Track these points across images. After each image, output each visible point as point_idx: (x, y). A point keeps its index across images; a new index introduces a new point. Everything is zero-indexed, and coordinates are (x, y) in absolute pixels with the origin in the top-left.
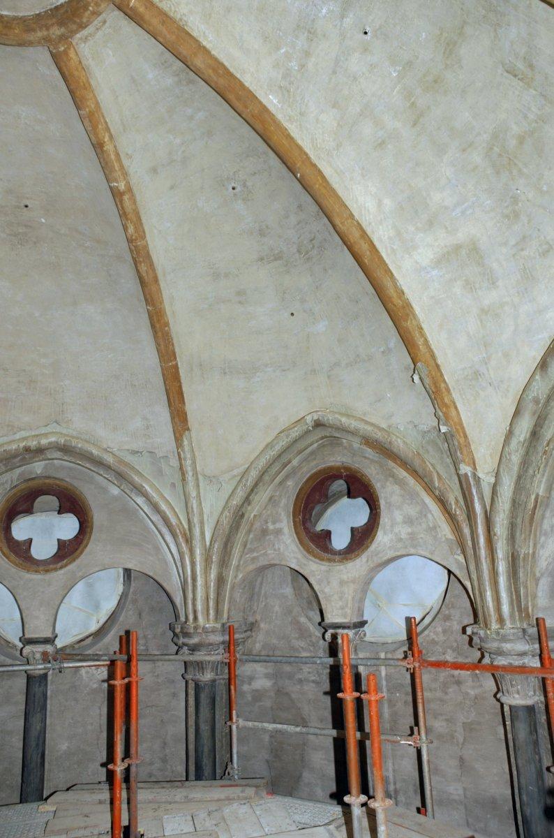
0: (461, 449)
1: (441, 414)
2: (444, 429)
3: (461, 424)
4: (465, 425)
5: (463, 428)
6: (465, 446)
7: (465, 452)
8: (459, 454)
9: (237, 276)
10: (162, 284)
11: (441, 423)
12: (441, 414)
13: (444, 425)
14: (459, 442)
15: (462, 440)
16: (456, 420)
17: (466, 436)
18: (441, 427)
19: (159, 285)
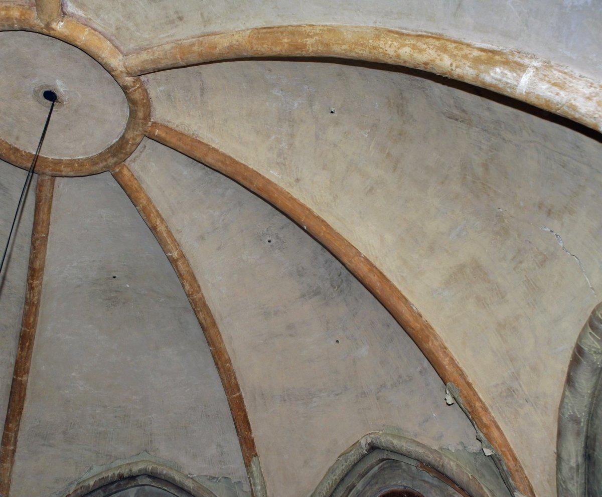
0: (512, 476)
1: (482, 435)
2: (488, 452)
3: (507, 445)
4: (512, 446)
5: (510, 450)
6: (517, 471)
7: (517, 478)
8: (510, 480)
9: (285, 312)
10: (221, 327)
11: (484, 445)
12: (482, 435)
13: (487, 447)
14: (508, 467)
15: (511, 464)
16: (499, 441)
17: (515, 459)
18: (485, 450)
19: (217, 328)
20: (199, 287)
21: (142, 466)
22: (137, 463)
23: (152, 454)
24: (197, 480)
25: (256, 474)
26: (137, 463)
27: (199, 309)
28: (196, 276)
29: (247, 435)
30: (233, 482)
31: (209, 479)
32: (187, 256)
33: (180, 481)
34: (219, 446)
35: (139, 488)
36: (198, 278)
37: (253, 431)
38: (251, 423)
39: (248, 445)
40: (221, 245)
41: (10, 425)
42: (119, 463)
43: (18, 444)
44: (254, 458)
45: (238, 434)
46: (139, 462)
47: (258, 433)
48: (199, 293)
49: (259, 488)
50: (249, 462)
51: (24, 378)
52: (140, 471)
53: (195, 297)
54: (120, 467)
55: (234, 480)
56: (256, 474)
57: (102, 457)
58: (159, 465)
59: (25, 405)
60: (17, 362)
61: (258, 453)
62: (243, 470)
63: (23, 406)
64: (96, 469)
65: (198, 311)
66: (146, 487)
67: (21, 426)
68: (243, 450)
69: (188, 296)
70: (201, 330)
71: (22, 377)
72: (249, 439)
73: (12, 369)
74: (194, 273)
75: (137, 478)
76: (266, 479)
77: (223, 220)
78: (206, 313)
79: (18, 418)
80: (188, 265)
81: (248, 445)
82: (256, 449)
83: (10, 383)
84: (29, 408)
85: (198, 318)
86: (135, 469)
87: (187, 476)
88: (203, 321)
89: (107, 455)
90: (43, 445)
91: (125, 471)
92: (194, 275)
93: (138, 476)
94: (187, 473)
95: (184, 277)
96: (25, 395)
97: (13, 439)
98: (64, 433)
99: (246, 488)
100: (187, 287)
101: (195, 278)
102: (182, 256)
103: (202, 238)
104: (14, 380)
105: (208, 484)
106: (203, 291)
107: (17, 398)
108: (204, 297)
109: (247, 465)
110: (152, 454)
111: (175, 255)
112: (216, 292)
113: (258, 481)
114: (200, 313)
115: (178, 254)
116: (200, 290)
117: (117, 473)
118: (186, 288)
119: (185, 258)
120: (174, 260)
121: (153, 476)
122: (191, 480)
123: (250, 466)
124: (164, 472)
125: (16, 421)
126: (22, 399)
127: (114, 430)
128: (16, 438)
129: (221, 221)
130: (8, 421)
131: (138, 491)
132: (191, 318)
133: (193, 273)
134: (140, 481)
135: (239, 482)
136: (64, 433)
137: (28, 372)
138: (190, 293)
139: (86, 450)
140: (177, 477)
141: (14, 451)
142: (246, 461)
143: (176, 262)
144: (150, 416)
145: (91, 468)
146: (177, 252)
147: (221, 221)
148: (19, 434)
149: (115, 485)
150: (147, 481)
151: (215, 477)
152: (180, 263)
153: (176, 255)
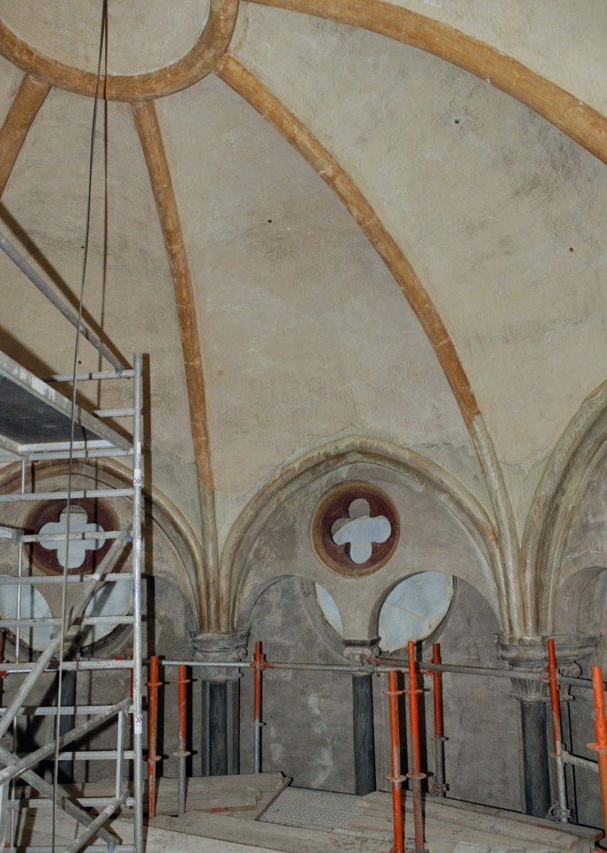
20: (371, 209)
21: (348, 442)
22: (342, 439)
23: (359, 427)
24: (414, 449)
25: (480, 435)
26: (342, 439)
27: (376, 239)
28: (365, 195)
29: (464, 391)
30: (455, 448)
31: (427, 447)
32: (347, 170)
33: (394, 454)
34: (434, 407)
35: (351, 465)
36: (367, 196)
37: (472, 385)
38: (468, 376)
39: (468, 403)
40: (391, 145)
41: (195, 415)
42: (323, 441)
43: (210, 433)
44: (476, 417)
45: (453, 391)
46: (344, 437)
47: (478, 386)
48: (372, 218)
49: (486, 450)
50: (470, 421)
51: (197, 362)
52: (347, 447)
53: (368, 223)
54: (325, 445)
55: (457, 446)
56: (480, 435)
57: (304, 437)
58: (368, 438)
59: (206, 392)
60: (183, 345)
61: (481, 410)
62: (465, 434)
63: (204, 393)
64: (300, 451)
65: (377, 243)
66: (358, 464)
67: (208, 414)
68: (461, 409)
69: (360, 224)
70: (386, 268)
71: (193, 361)
72: (466, 395)
73: (181, 355)
74: (361, 192)
75: (346, 455)
76: (494, 440)
77: (386, 105)
78: (386, 243)
79: (202, 407)
80: (351, 182)
81: (468, 403)
82: (478, 405)
83: (184, 371)
84: (211, 395)
85: (378, 252)
86: (342, 447)
87: (401, 447)
88: (385, 254)
89: (309, 435)
90: (237, 432)
91: (331, 450)
92: (361, 195)
93: (346, 453)
94: (402, 443)
95: (348, 199)
96: (203, 380)
97: (202, 430)
98: (256, 416)
99: (472, 452)
100: (355, 212)
101: (364, 198)
102: (340, 170)
103: (363, 139)
104: (187, 366)
105: (427, 453)
106: (378, 213)
107: (194, 386)
108: (380, 222)
109: (469, 426)
110: (359, 427)
111: (329, 171)
112: (395, 217)
113: (483, 443)
114: (379, 244)
115: (332, 169)
116: (374, 214)
117: (322, 452)
118: (354, 214)
119: (344, 173)
120: (330, 179)
121: (364, 452)
122: (406, 451)
123: (472, 426)
124: (375, 445)
125: (201, 411)
126: (201, 386)
127: (311, 406)
128: (205, 428)
129: (383, 108)
130: (192, 412)
131: (350, 469)
132: (371, 253)
133: (359, 192)
134: (350, 458)
135: (463, 447)
136: (256, 416)
137: (199, 355)
138: (360, 219)
139: (284, 431)
140: (390, 449)
141: (207, 442)
142: (467, 422)
143: (333, 181)
144: (349, 385)
145: (293, 451)
146: (331, 166)
147: (383, 108)
148: (208, 424)
149: (323, 466)
150: (358, 457)
151: (434, 445)
152: (338, 181)
153: (331, 172)
